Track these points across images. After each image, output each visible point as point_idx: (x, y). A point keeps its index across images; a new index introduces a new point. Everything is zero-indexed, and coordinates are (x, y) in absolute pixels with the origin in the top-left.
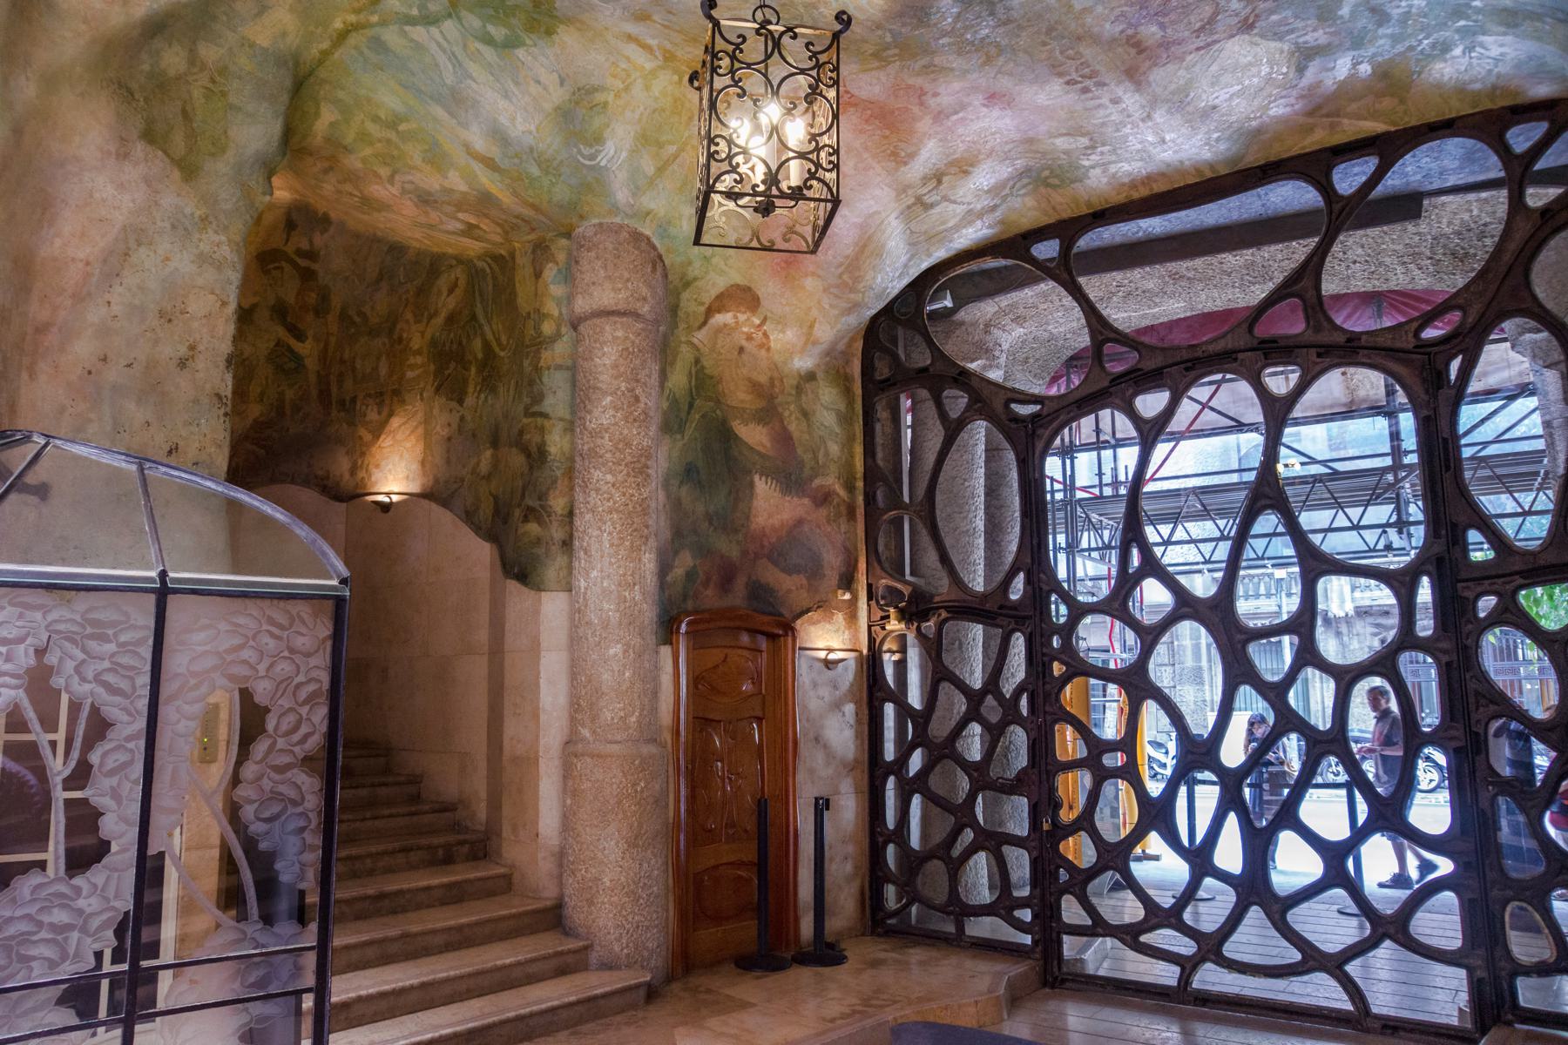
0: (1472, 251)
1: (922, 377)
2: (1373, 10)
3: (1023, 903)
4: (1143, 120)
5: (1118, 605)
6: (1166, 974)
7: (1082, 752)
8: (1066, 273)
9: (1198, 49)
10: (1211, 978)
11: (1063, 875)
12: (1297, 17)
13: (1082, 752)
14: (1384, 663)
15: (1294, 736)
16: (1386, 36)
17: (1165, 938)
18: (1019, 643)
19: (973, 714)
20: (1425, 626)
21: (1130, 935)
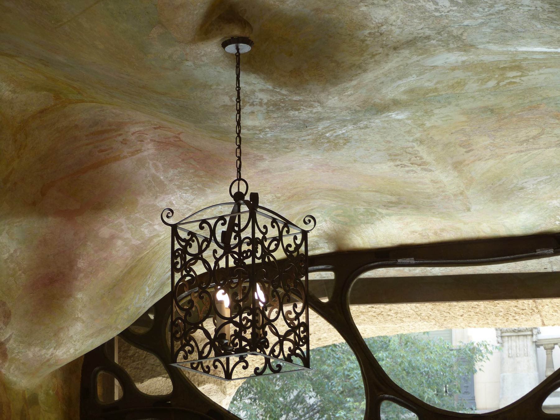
9: (518, 152)
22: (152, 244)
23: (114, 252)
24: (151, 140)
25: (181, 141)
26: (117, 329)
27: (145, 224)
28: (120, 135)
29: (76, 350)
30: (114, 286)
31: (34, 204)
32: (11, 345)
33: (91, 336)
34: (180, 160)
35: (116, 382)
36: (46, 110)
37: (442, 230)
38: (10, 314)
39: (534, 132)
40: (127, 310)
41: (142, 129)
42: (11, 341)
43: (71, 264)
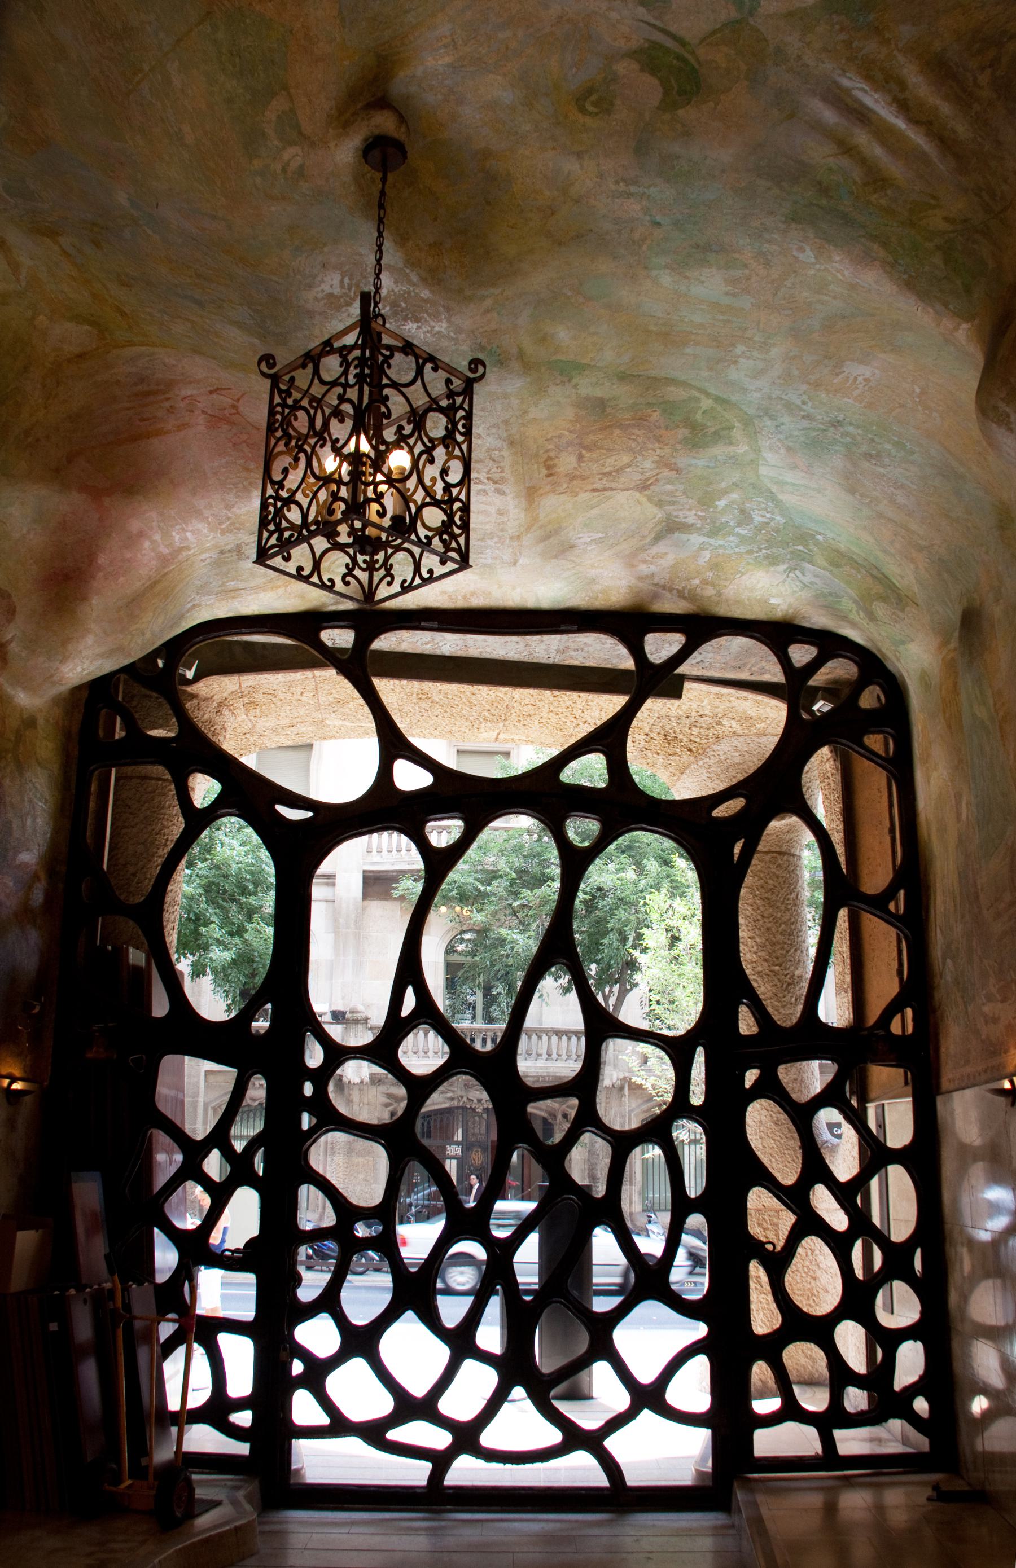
0: (680, 736)
1: (158, 751)
2: (742, 511)
3: (240, 1404)
4: (511, 538)
6: (415, 1473)
7: (329, 1219)
8: (360, 669)
9: (594, 490)
10: (466, 1471)
11: (297, 1367)
12: (684, 493)
13: (329, 1219)
14: (657, 1130)
15: (693, 1196)
16: (738, 534)
17: (418, 1432)
18: (257, 1090)
20: (697, 1097)
21: (373, 1433)
22: (180, 557)
23: (139, 556)
24: (203, 412)
25: (238, 413)
26: (130, 655)
27: (178, 527)
28: (168, 399)
29: (83, 669)
30: (133, 600)
31: (57, 471)
32: (14, 648)
33: (101, 655)
34: (231, 445)
35: (118, 719)
36: (85, 353)
37: (473, 594)
38: (14, 611)
39: (626, 459)
40: (143, 634)
41: (195, 392)
42: (13, 645)
43: (92, 557)
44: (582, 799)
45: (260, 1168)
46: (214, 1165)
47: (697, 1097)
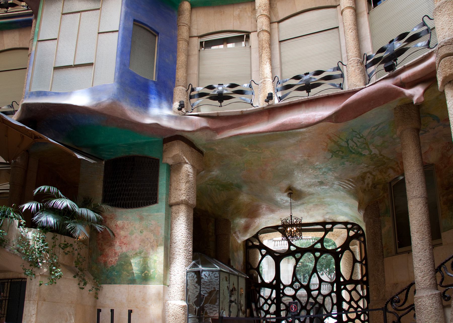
5: (291, 286)
14: (329, 295)
19: (266, 302)
20: (335, 290)
44: (318, 250)
45: (275, 301)
46: (269, 302)
47: (335, 290)
